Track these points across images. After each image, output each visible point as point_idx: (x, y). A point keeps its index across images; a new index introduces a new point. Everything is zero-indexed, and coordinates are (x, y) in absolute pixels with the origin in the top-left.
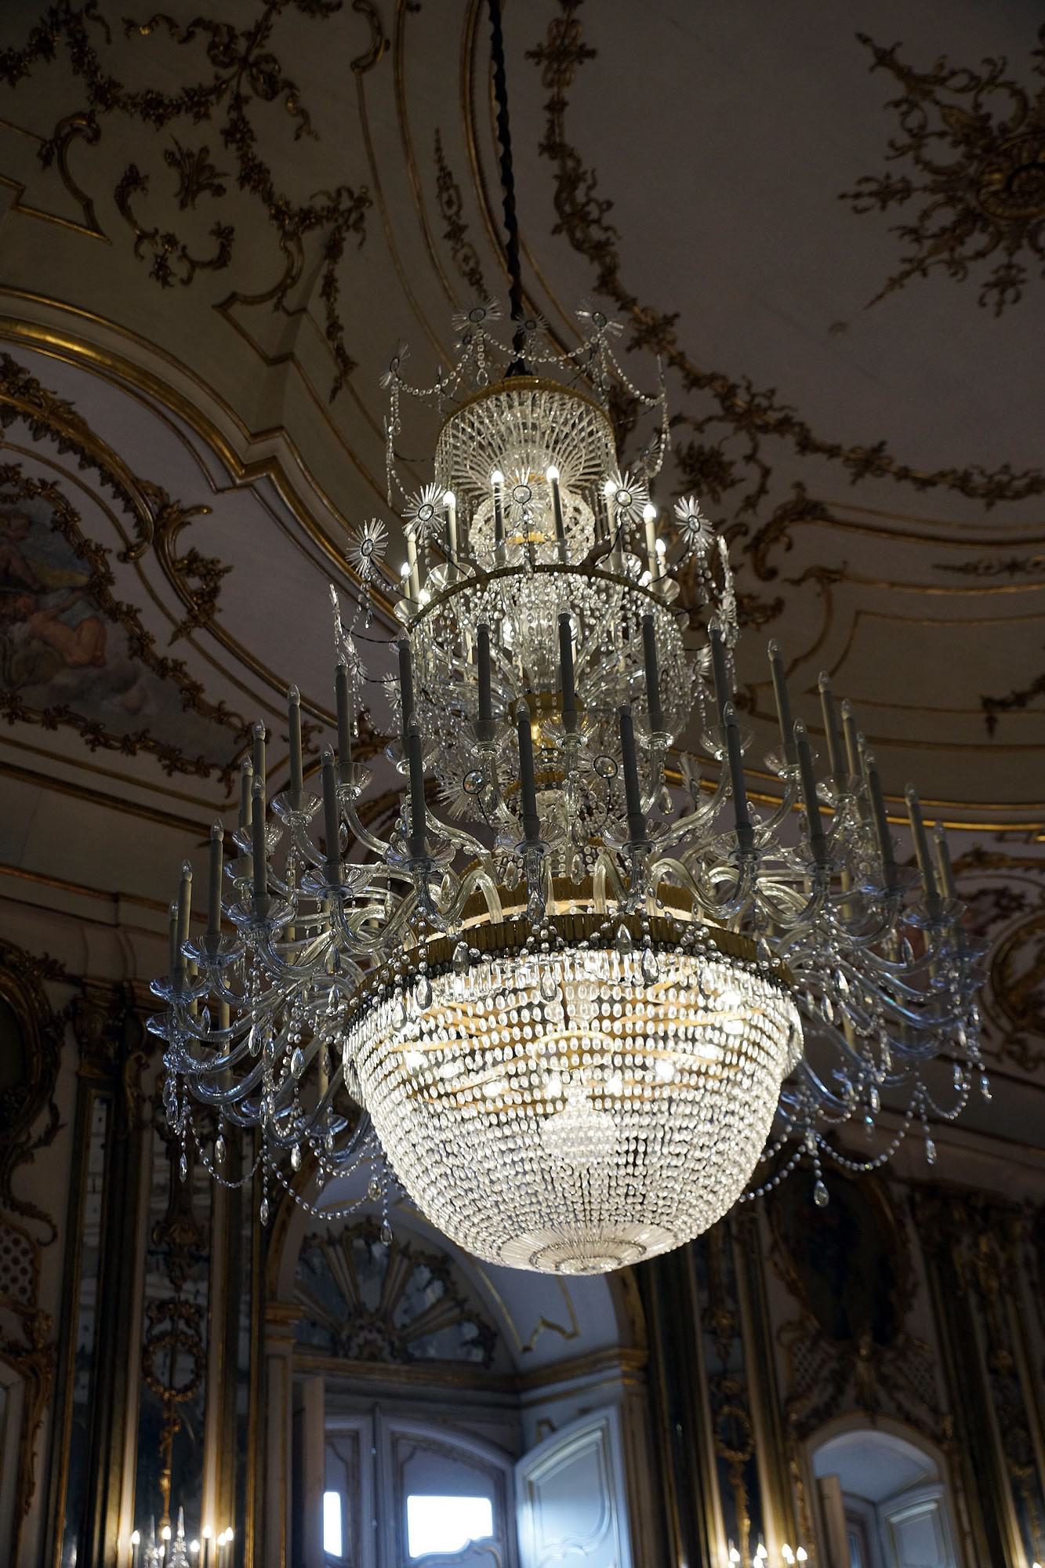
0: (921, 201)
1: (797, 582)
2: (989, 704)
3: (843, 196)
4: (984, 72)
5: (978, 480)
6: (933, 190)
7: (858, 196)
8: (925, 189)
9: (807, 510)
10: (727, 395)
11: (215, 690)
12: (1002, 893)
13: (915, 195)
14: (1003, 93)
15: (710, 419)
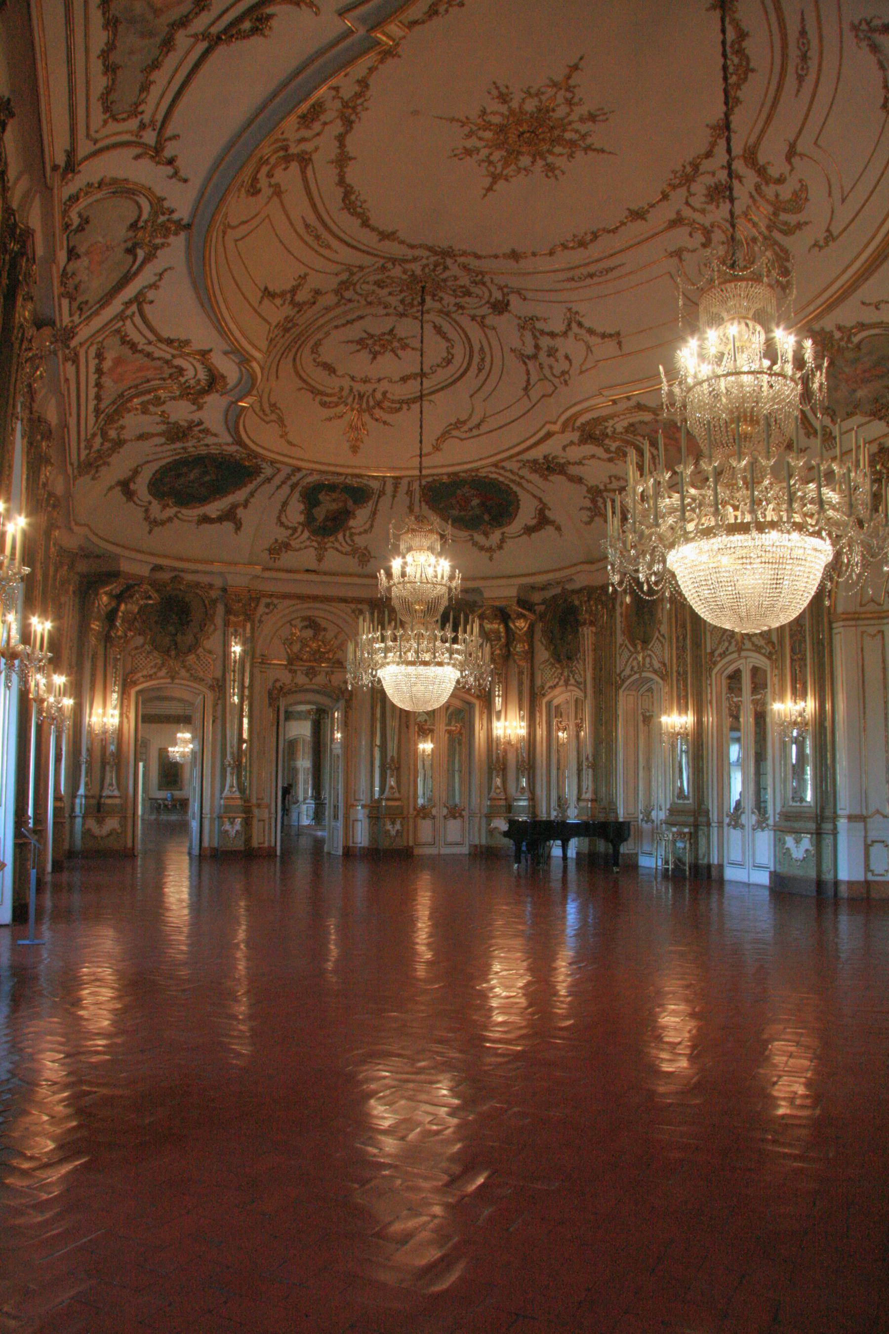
0: (504, 109)
1: (270, 186)
2: (266, 289)
3: (494, 83)
4: (576, 100)
5: (353, 197)
6: (510, 110)
7: (497, 88)
8: (509, 107)
9: (304, 160)
10: (358, 95)
11: (160, 77)
12: (181, 371)
13: (506, 106)
14: (568, 110)
15: (342, 98)
